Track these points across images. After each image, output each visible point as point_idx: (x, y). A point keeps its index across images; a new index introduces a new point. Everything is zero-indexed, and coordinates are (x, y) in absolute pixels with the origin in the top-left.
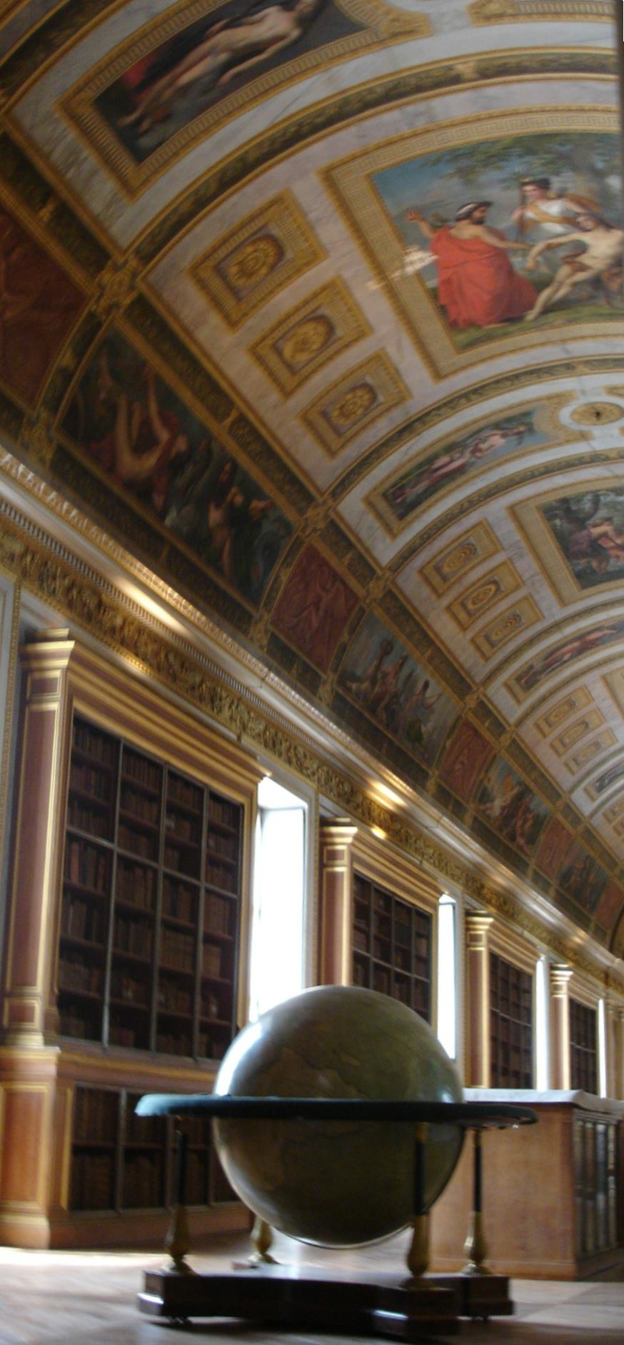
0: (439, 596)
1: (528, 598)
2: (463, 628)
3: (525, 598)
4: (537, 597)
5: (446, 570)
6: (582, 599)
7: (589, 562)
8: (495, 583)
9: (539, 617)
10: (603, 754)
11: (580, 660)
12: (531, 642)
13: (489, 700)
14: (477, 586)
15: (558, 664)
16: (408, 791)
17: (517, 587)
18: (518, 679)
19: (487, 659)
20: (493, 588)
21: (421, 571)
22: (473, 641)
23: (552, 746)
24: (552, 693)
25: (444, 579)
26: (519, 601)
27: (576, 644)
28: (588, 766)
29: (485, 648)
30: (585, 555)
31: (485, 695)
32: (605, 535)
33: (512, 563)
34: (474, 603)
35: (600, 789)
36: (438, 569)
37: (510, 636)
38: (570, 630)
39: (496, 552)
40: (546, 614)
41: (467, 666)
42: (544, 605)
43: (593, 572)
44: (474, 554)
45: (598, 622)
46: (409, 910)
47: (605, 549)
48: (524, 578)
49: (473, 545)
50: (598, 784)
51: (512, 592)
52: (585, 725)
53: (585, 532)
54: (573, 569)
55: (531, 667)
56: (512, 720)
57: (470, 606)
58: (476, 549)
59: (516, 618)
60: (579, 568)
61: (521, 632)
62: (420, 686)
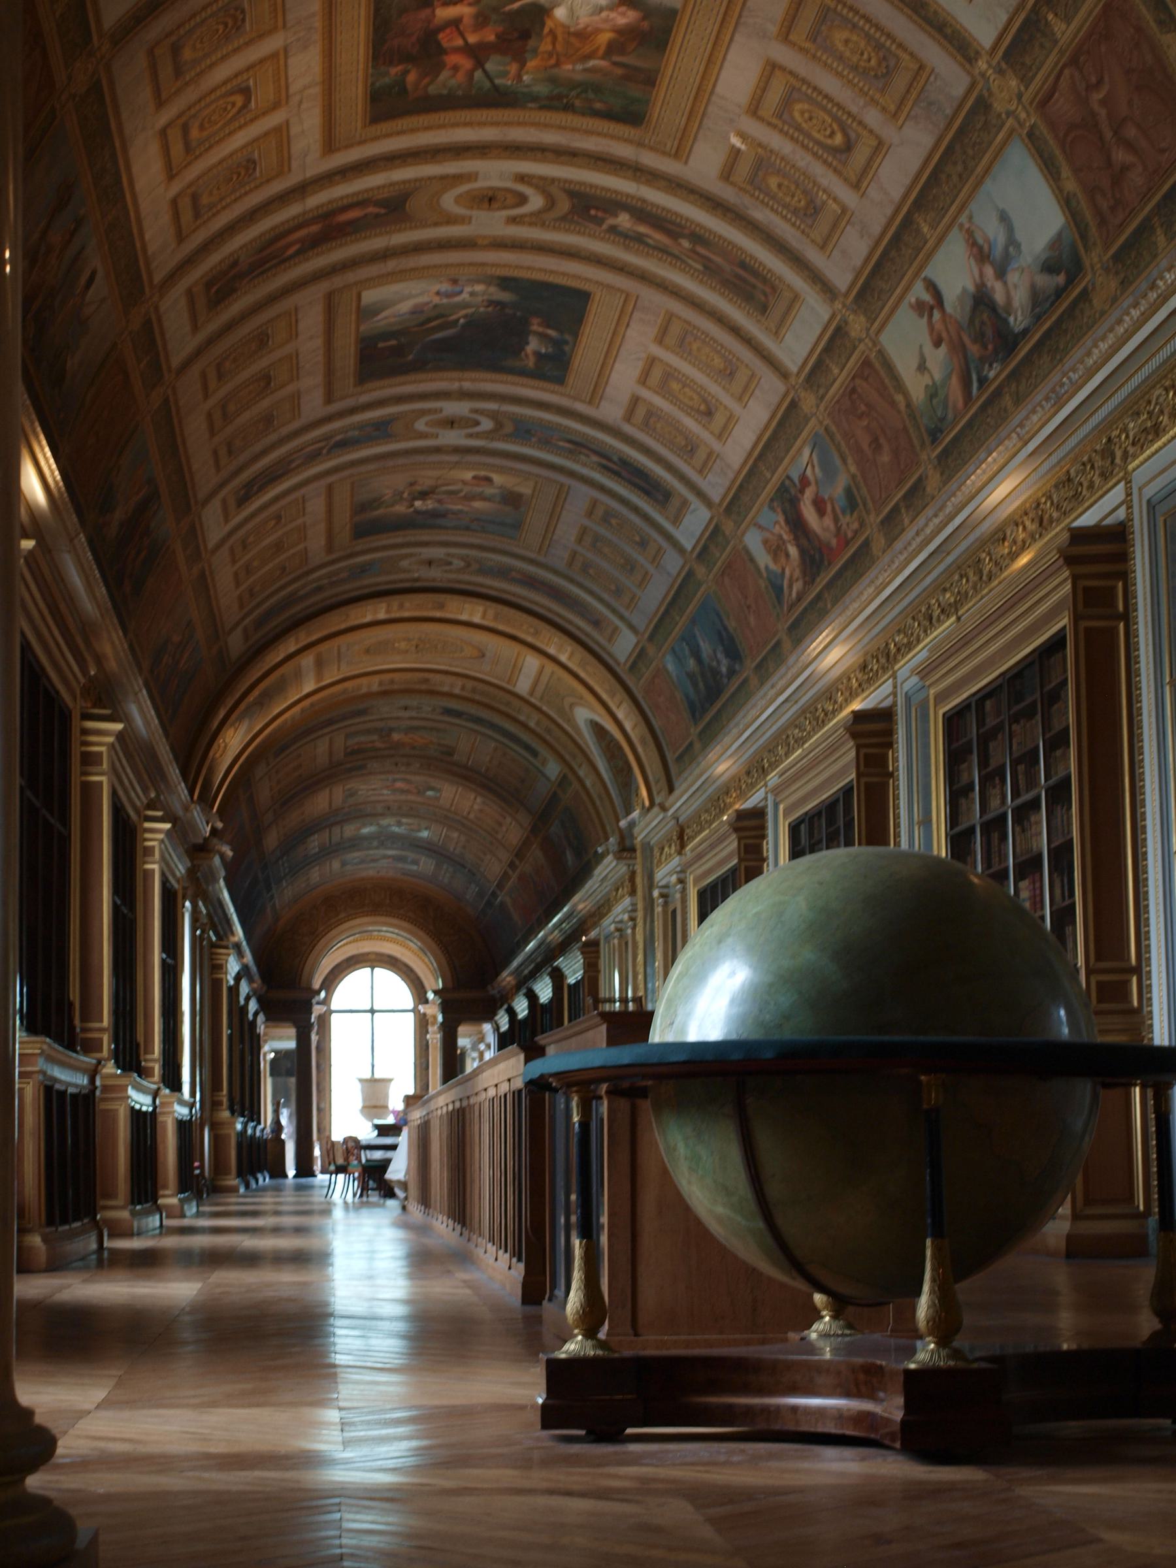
0: (160, 103)
1: (281, 133)
2: (171, 174)
3: (277, 130)
4: (295, 130)
5: (187, 54)
6: (362, 142)
7: (406, 72)
8: (246, 92)
9: (284, 166)
10: (273, 437)
11: (307, 260)
12: (252, 216)
13: (159, 320)
14: (218, 93)
15: (274, 262)
16: (54, 479)
17: (276, 106)
18: (208, 285)
19: (181, 238)
20: (239, 100)
21: (151, 52)
22: (174, 202)
23: (209, 415)
24: (244, 316)
25: (178, 72)
26: (266, 134)
27: (315, 228)
28: (242, 458)
29: (187, 216)
30: (406, 58)
31: (157, 309)
32: (456, 23)
33: (286, 58)
34: (202, 128)
35: (243, 499)
36: (176, 50)
37: (228, 200)
38: (317, 200)
39: (273, 30)
40: (294, 165)
41: (151, 249)
42: (297, 147)
43: (403, 89)
44: (238, 29)
45: (367, 191)
46: (52, 698)
47: (442, 51)
48: (292, 90)
49: (243, 11)
50: (242, 492)
51: (264, 114)
52: (265, 380)
53: (424, 13)
54: (373, 84)
55: (235, 263)
56: (176, 362)
57: (195, 133)
58: (243, 20)
59: (251, 164)
60: (387, 80)
61: (246, 193)
62: (83, 280)
